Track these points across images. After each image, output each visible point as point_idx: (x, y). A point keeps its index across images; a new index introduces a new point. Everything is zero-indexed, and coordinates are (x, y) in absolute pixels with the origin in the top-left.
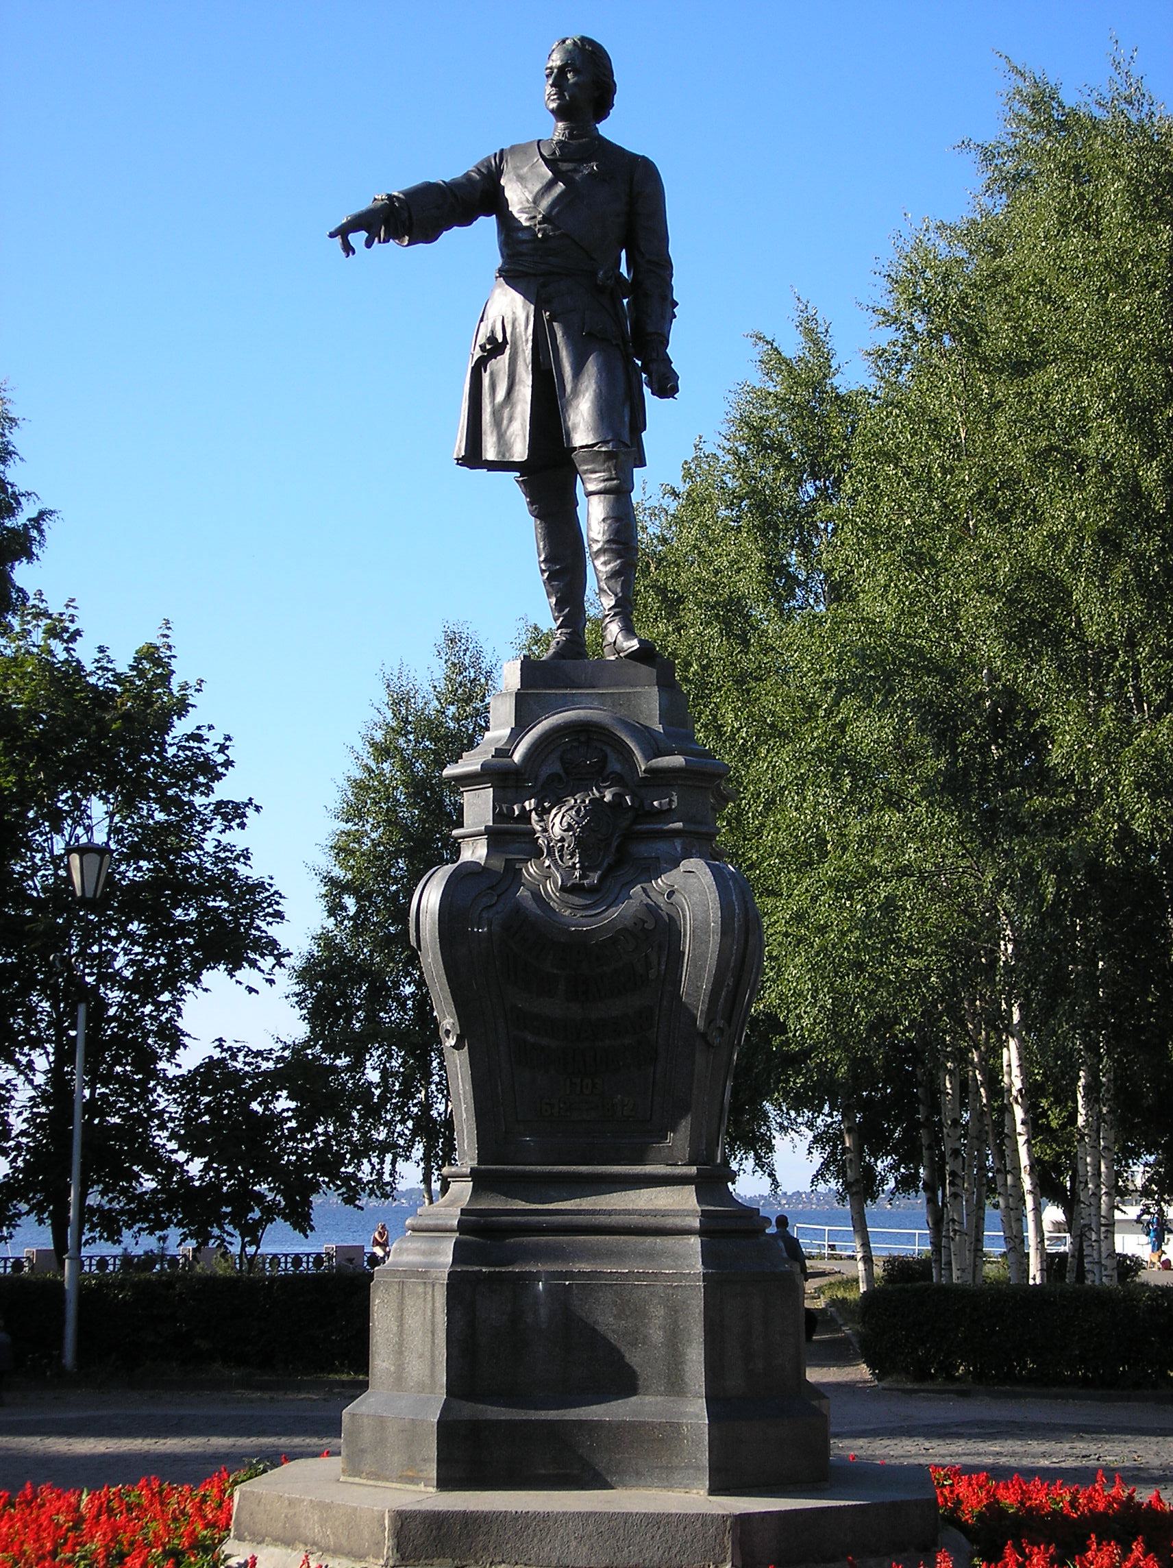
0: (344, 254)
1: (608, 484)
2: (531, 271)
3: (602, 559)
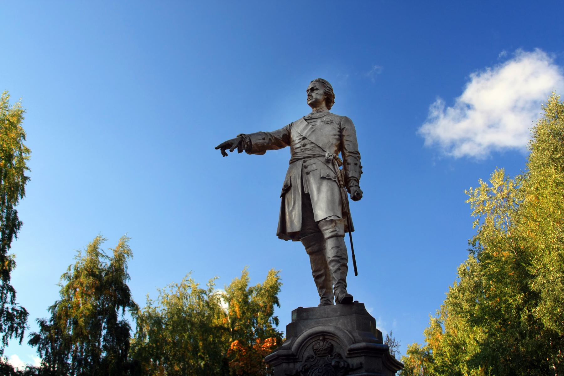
0: (222, 156)
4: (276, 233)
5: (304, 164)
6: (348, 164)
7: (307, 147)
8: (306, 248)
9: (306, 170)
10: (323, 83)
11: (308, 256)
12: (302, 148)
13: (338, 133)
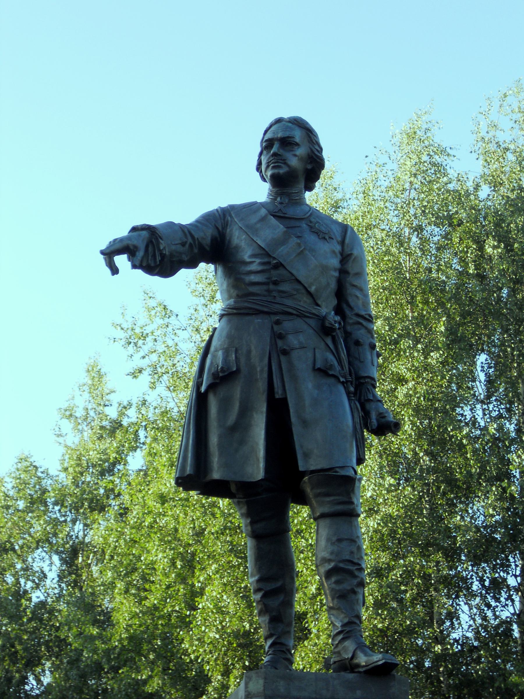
2: (266, 309)
3: (333, 579)
6: (358, 343)
12: (272, 287)
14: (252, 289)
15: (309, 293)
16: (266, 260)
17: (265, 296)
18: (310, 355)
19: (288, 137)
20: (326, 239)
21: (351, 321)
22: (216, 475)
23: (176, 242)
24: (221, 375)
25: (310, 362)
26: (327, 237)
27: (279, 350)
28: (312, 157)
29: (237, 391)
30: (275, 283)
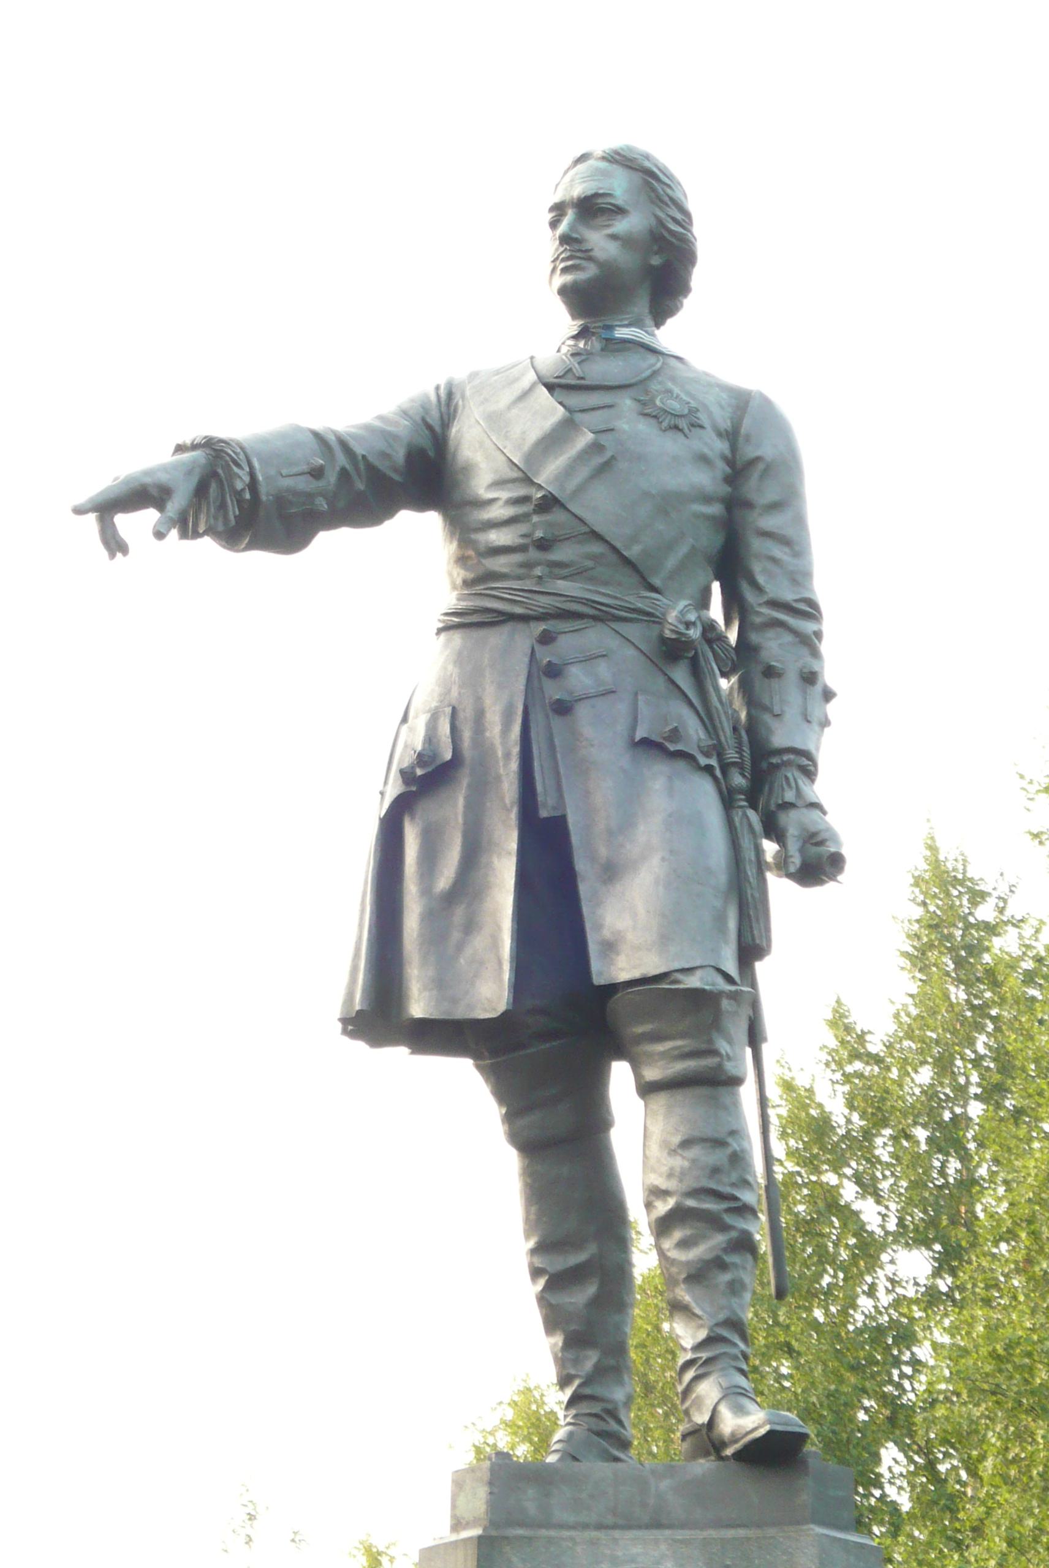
0: (104, 553)
1: (691, 1064)
2: (518, 610)
3: (678, 1235)
4: (336, 1010)
5: (545, 656)
6: (770, 672)
7: (560, 554)
8: (510, 1118)
9: (553, 691)
10: (651, 181)
11: (509, 1163)
12: (533, 554)
13: (726, 489)
14: (500, 564)
15: (627, 561)
16: (520, 491)
17: (519, 578)
18: (622, 708)
19: (596, 195)
20: (681, 430)
21: (758, 620)
22: (418, 1009)
23: (295, 470)
24: (419, 772)
25: (622, 727)
26: (683, 424)
27: (547, 705)
28: (663, 238)
29: (453, 807)
30: (543, 545)
